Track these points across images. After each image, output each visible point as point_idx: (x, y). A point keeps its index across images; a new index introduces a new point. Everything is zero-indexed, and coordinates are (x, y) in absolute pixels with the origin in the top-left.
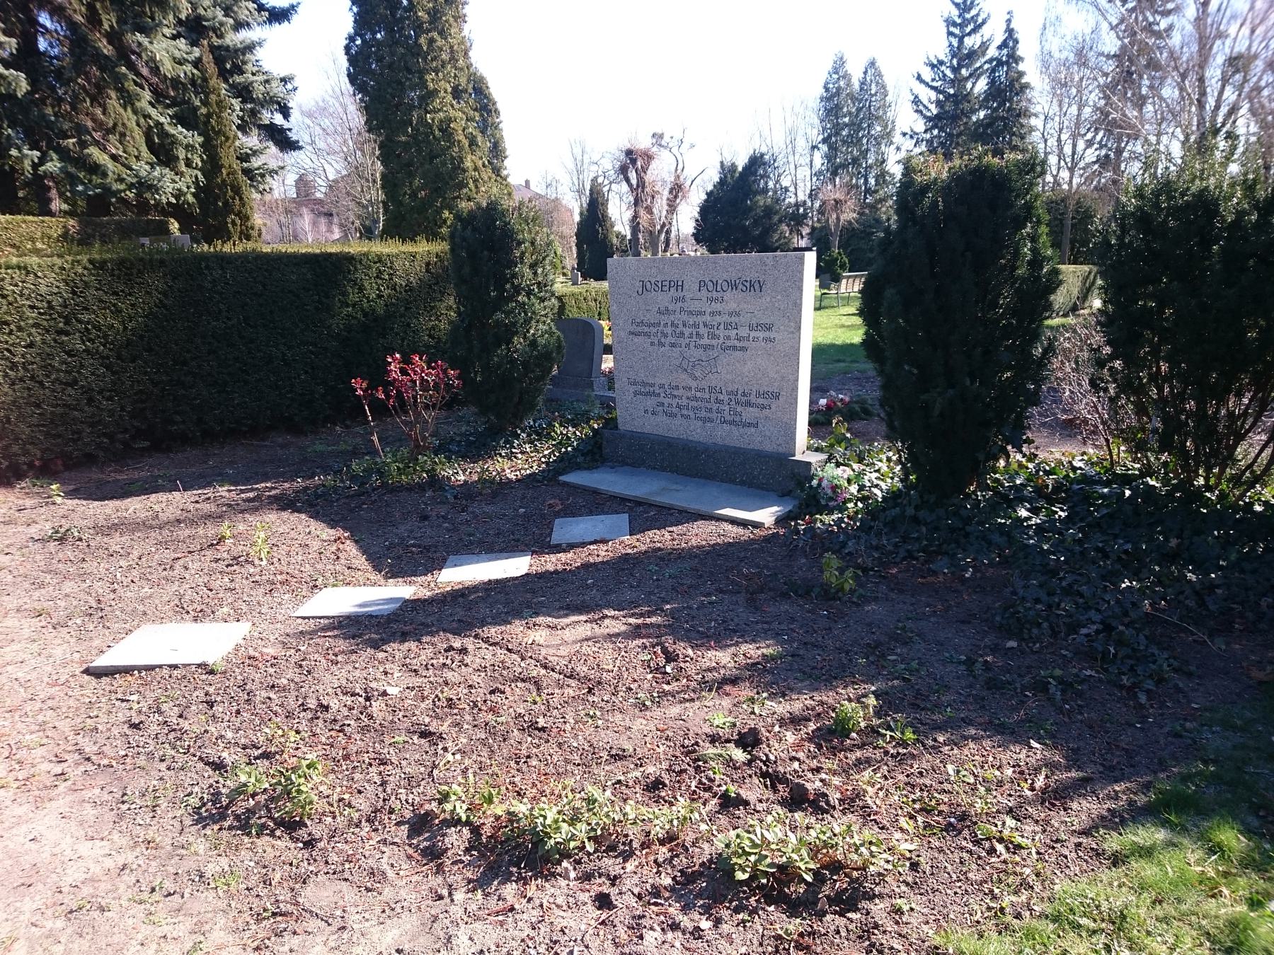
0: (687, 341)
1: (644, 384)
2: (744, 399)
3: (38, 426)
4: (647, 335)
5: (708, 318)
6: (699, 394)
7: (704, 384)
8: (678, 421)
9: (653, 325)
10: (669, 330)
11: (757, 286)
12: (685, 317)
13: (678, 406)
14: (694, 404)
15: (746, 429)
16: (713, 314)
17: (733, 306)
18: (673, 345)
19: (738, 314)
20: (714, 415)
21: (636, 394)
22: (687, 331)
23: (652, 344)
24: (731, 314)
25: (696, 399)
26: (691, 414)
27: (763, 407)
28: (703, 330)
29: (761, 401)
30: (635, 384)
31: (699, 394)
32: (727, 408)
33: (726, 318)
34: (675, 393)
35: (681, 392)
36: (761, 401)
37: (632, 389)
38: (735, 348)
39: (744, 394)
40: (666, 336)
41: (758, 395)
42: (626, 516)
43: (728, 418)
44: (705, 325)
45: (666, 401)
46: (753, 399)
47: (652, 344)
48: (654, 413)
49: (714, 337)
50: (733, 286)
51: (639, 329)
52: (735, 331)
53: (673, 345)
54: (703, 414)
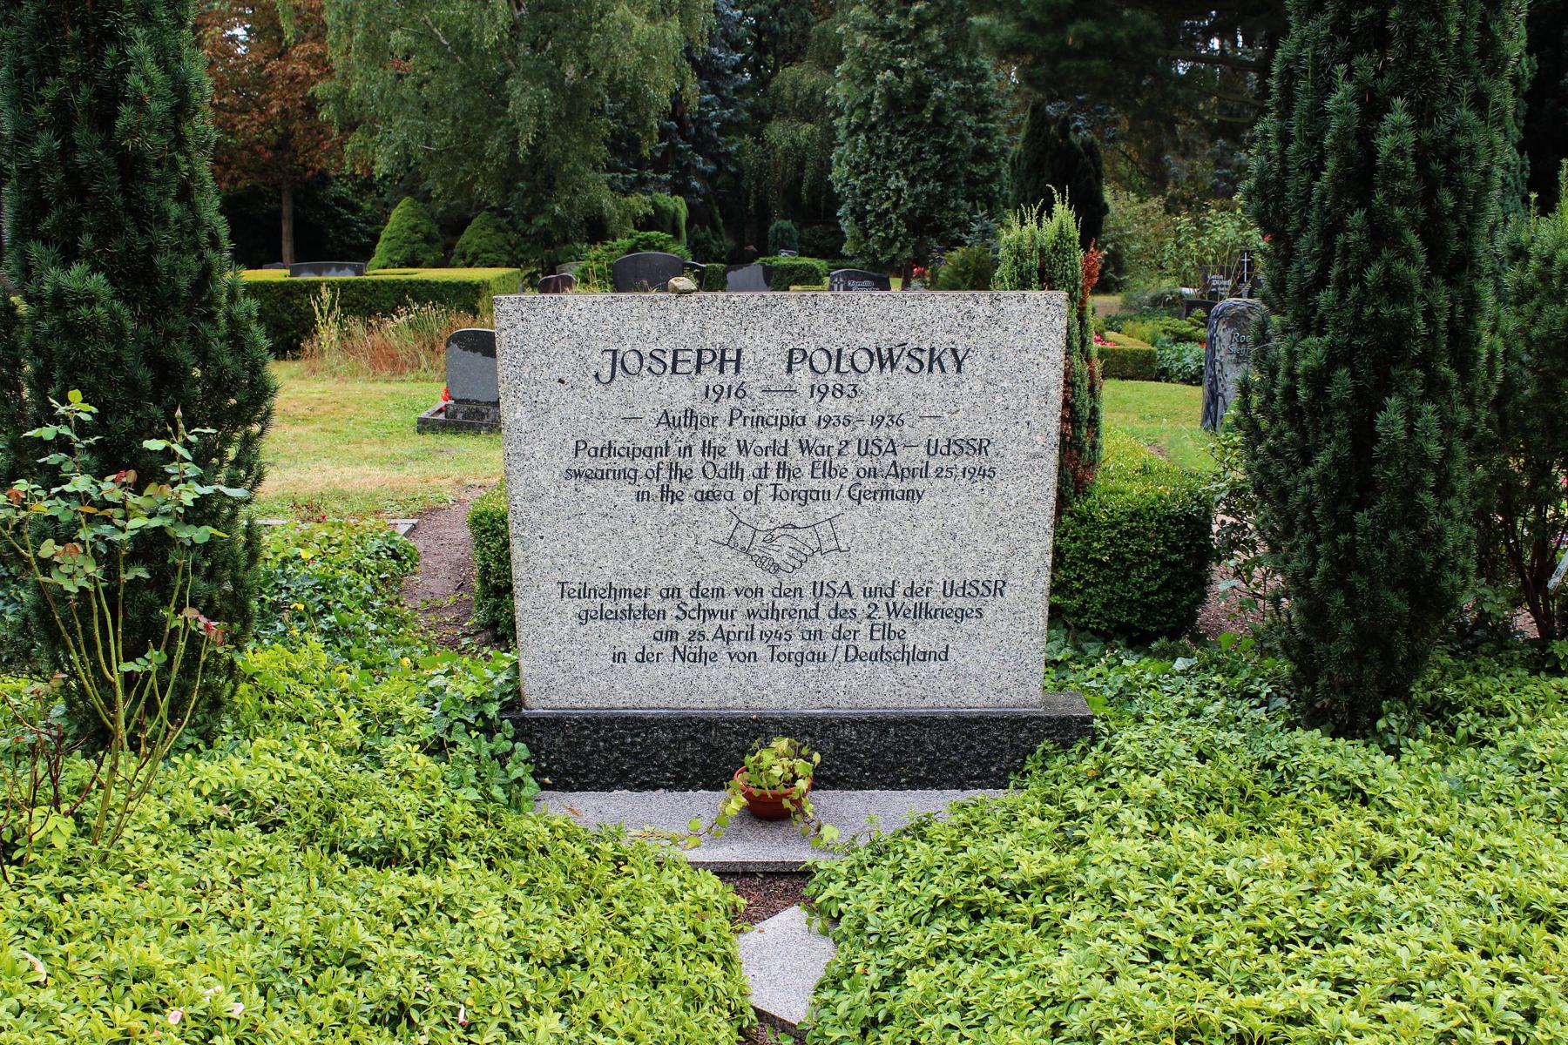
0: (751, 484)
1: (613, 592)
2: (910, 603)
3: (91, 646)
4: (621, 474)
5: (811, 432)
6: (782, 603)
7: (803, 579)
8: (716, 671)
9: (647, 452)
10: (696, 462)
11: (948, 361)
12: (741, 431)
13: (725, 637)
14: (771, 625)
15: (917, 667)
16: (825, 422)
17: (878, 404)
18: (706, 497)
19: (898, 422)
20: (827, 646)
21: (585, 617)
22: (750, 464)
23: (640, 496)
24: (877, 422)
25: (774, 613)
26: (761, 648)
27: (963, 614)
28: (796, 458)
29: (957, 602)
30: (584, 592)
31: (782, 603)
32: (864, 627)
33: (864, 430)
34: (713, 605)
35: (730, 601)
36: (957, 602)
37: (572, 607)
38: (888, 494)
39: (912, 591)
40: (685, 476)
41: (949, 589)
42: (1063, 294)
43: (866, 646)
44: (805, 447)
45: (685, 627)
46: (935, 600)
47: (640, 496)
48: (643, 658)
49: (829, 471)
50: (884, 359)
51: (603, 464)
52: (890, 458)
53: (706, 497)
54: (797, 645)
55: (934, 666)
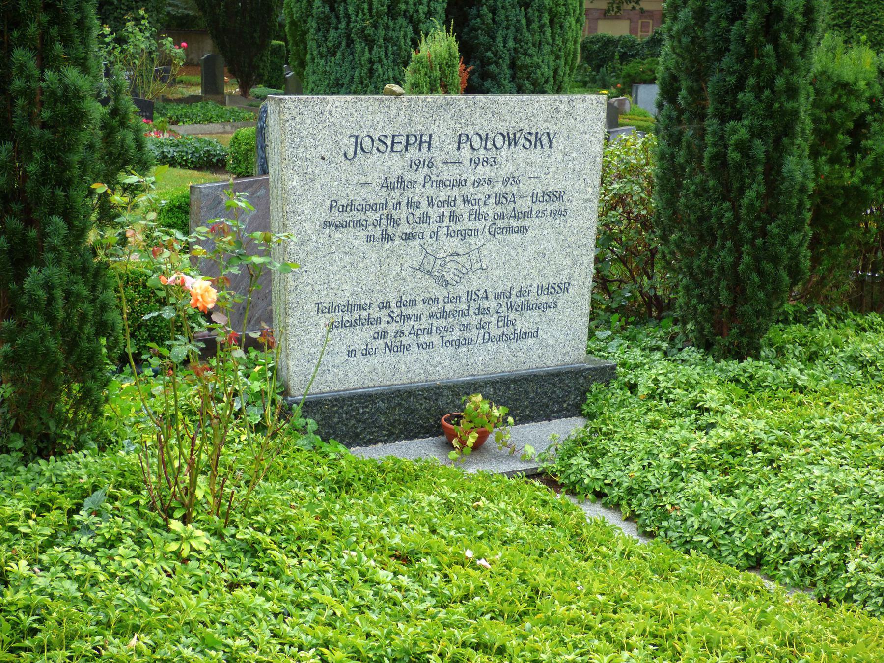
0: (434, 227)
1: (350, 307)
2: (519, 301)
4: (361, 224)
6: (449, 307)
7: (461, 290)
8: (408, 357)
9: (373, 208)
11: (545, 141)
12: (430, 191)
13: (415, 332)
14: (442, 322)
15: (523, 344)
16: (478, 183)
17: (506, 170)
18: (408, 237)
19: (516, 181)
20: (472, 334)
21: (332, 326)
22: (434, 213)
23: (369, 238)
24: (505, 182)
25: (444, 314)
26: (436, 339)
28: (462, 209)
29: (544, 298)
30: (332, 309)
32: (494, 319)
33: (499, 188)
34: (409, 312)
36: (544, 298)
37: (324, 320)
38: (510, 230)
39: (520, 294)
40: (396, 223)
41: (541, 290)
44: (465, 200)
45: (392, 328)
46: (532, 298)
47: (369, 238)
48: (367, 353)
49: (479, 216)
50: (511, 140)
52: (512, 205)
53: (408, 237)
54: (456, 334)
55: (531, 341)
